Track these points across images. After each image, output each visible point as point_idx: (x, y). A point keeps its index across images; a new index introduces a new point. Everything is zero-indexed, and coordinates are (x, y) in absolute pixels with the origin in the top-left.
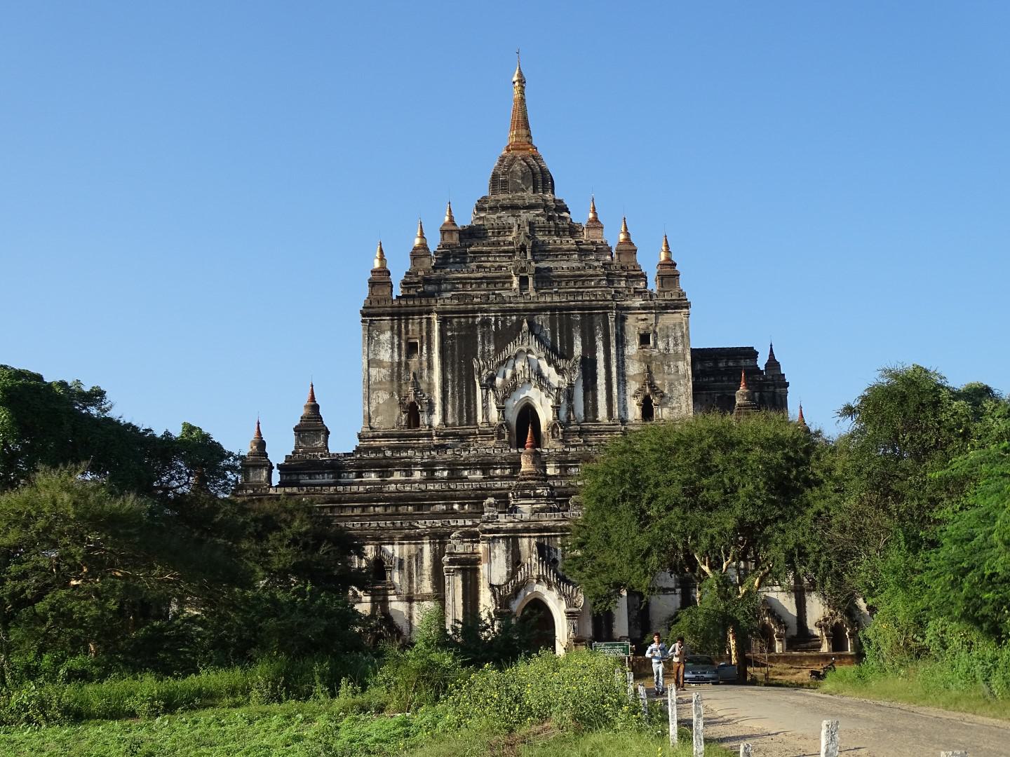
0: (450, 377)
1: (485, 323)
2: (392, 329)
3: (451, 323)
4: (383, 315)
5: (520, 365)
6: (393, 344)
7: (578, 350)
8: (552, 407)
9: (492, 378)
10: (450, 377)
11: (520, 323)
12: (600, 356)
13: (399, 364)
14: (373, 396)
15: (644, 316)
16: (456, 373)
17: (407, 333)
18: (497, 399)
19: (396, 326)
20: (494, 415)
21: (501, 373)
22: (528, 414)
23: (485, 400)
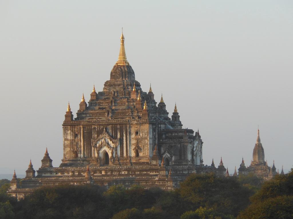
0: (85, 144)
1: (95, 128)
2: (71, 130)
3: (86, 128)
4: (68, 126)
5: (103, 140)
6: (71, 134)
7: (119, 136)
8: (111, 153)
9: (96, 144)
10: (85, 144)
11: (103, 128)
12: (124, 138)
13: (73, 140)
14: (66, 149)
15: (137, 127)
16: (87, 143)
17: (74, 131)
18: (97, 151)
19: (72, 129)
20: (96, 155)
21: (98, 143)
22: (106, 154)
23: (94, 151)
